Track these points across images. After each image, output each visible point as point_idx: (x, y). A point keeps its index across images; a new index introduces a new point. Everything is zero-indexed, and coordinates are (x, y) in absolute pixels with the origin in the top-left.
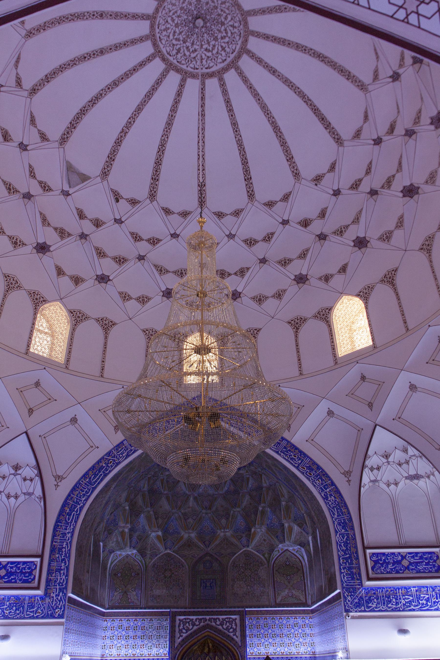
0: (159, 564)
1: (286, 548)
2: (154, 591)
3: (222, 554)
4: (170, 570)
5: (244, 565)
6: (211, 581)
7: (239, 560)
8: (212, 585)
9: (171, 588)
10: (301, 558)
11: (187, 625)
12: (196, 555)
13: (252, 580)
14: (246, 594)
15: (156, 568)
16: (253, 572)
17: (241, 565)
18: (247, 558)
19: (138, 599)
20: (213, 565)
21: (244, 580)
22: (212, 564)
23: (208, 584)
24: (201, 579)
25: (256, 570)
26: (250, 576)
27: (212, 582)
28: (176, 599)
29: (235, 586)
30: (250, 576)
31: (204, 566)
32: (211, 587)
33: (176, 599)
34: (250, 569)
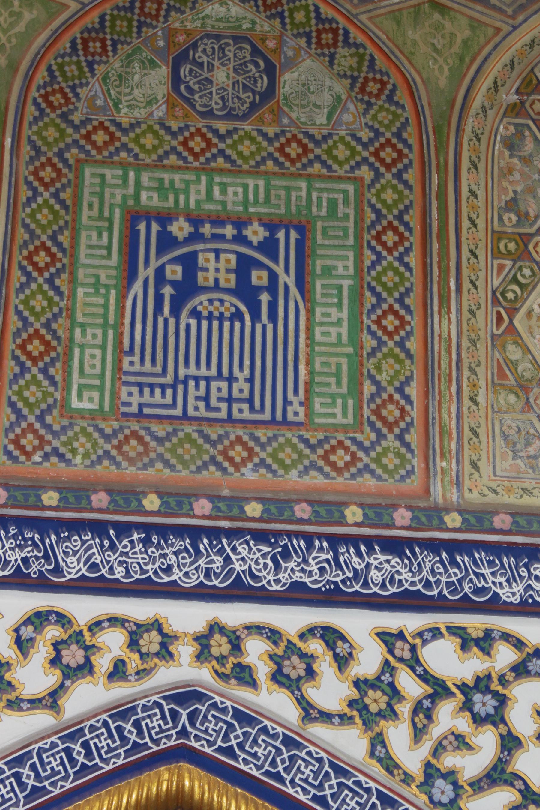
6: (256, 233)
20: (288, 81)
22: (271, 71)
23: (216, 267)
24: (134, 217)
27: (269, 247)
31: (176, 80)
32: (245, 291)
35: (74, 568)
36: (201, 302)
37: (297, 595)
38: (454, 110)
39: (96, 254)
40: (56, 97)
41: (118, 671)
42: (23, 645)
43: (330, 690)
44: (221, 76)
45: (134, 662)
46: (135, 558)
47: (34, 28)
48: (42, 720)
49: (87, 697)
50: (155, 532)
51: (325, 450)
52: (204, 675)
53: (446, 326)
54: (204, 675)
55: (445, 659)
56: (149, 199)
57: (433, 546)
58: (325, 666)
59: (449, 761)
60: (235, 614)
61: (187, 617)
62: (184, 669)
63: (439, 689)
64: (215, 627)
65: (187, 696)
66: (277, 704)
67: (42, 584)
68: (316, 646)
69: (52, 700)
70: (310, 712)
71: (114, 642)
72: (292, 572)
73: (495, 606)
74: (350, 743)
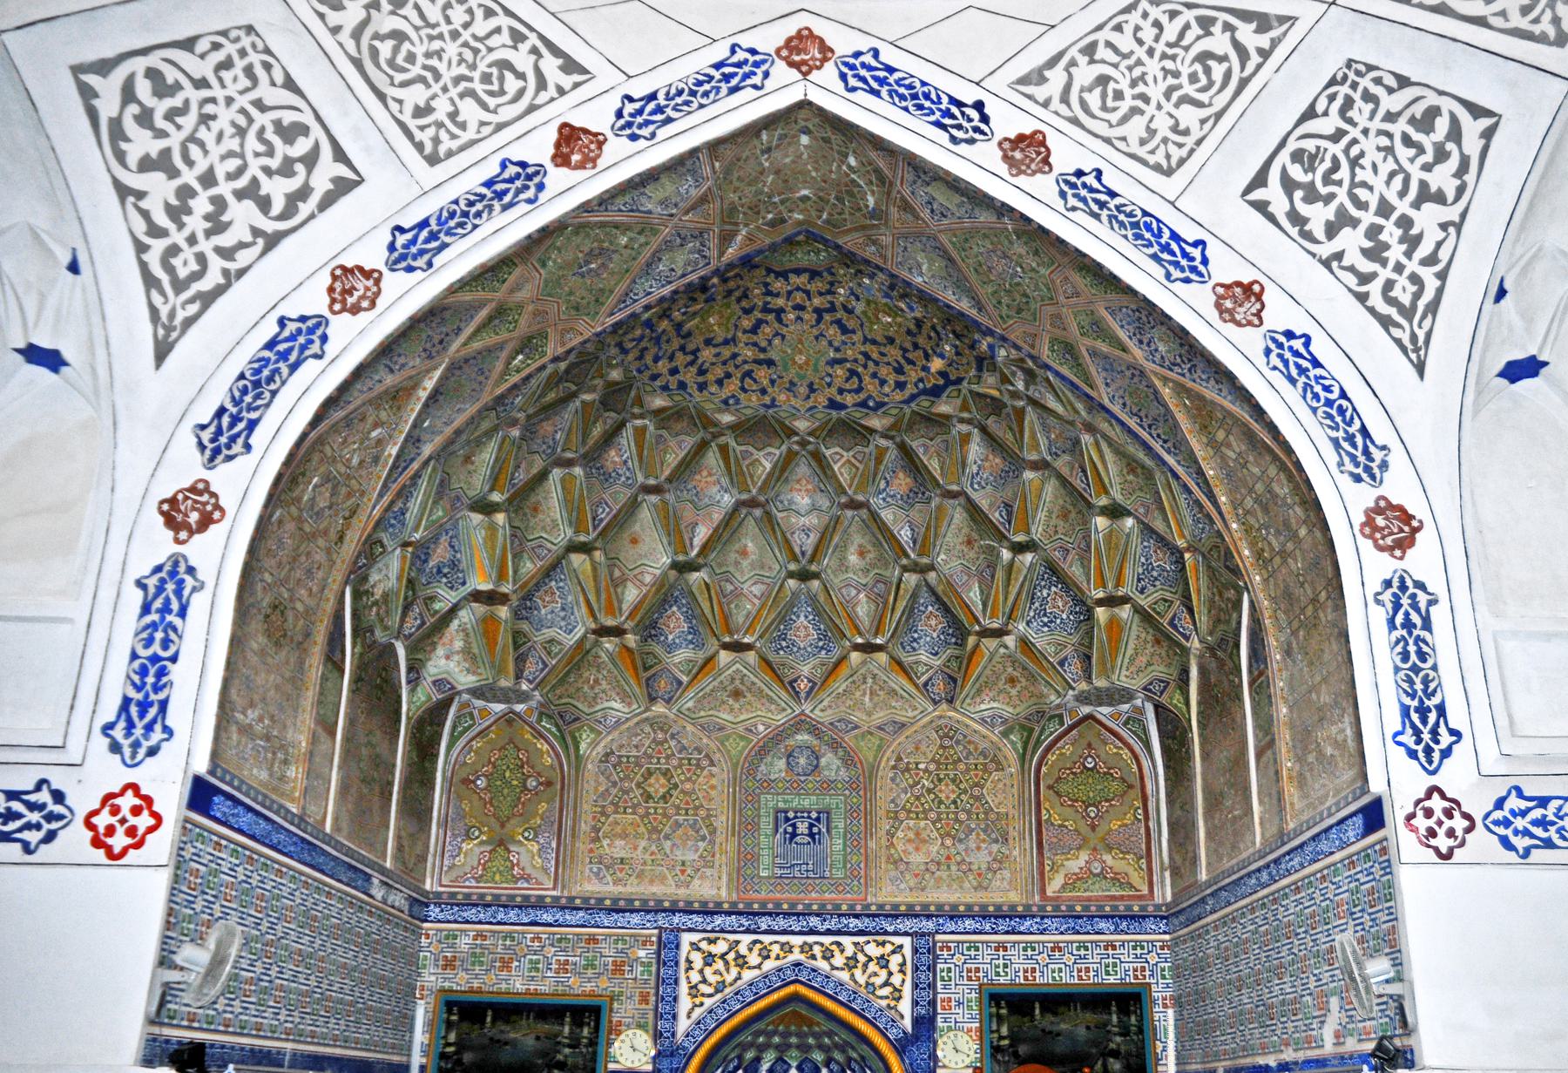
0: (623, 753)
1: (1086, 710)
2: (605, 842)
3: (857, 727)
4: (666, 773)
5: (932, 767)
6: (814, 815)
7: (917, 748)
8: (815, 830)
9: (667, 837)
10: (1138, 747)
11: (719, 965)
12: (761, 728)
13: (963, 816)
14: (938, 864)
15: (614, 767)
16: (965, 791)
17: (922, 766)
18: (947, 743)
19: (545, 870)
20: (823, 761)
21: (933, 815)
22: (817, 758)
23: (802, 828)
25: (976, 785)
26: (954, 802)
27: (818, 819)
28: (683, 872)
29: (900, 834)
30: (954, 802)
32: (811, 835)
33: (683, 872)
34: (953, 781)
35: (764, 927)
36: (798, 839)
37: (829, 932)
38: (873, 770)
39: (766, 824)
40: (752, 771)
41: (778, 958)
42: (750, 950)
43: (839, 960)
44: (802, 761)
45: (782, 954)
46: (781, 923)
47: (744, 748)
48: (756, 972)
49: (769, 965)
50: (787, 915)
51: (837, 886)
52: (802, 957)
53: (872, 844)
54: (802, 957)
55: (873, 950)
56: (781, 805)
57: (868, 916)
58: (837, 953)
59: (873, 980)
60: (811, 939)
61: (797, 940)
62: (796, 956)
63: (870, 959)
64: (805, 943)
65: (798, 964)
66: (822, 965)
67: (755, 932)
68: (834, 947)
69: (759, 967)
70: (834, 968)
71: (776, 949)
72: (826, 926)
73: (886, 933)
74: (844, 976)
